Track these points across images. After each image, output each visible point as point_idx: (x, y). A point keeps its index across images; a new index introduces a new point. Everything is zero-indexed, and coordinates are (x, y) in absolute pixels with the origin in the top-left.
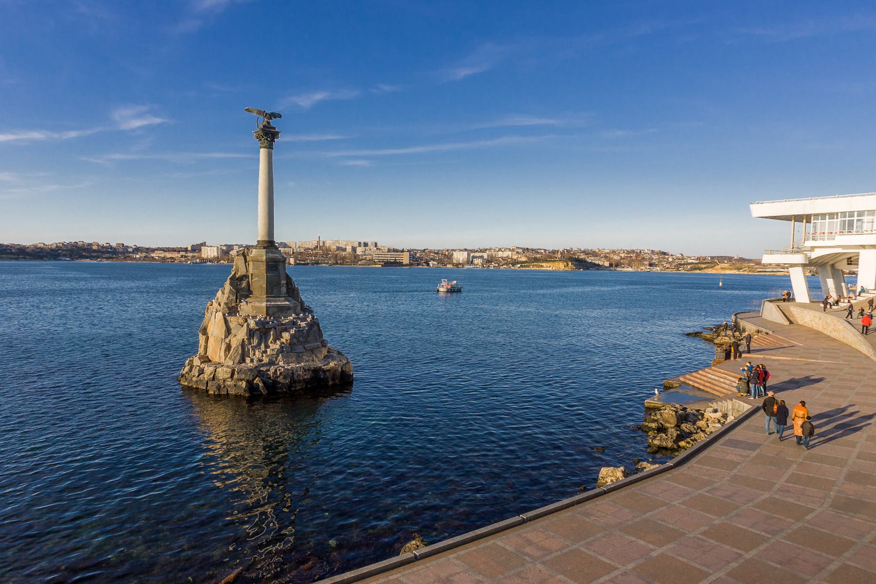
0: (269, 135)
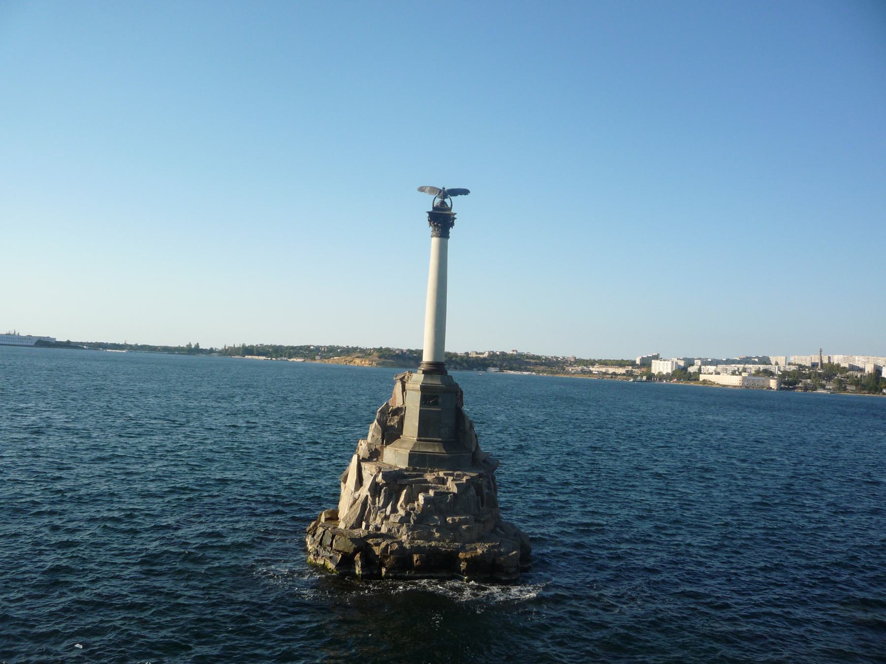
0: (442, 221)
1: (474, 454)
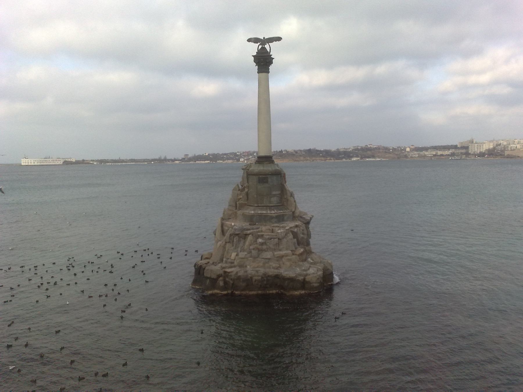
0: (263, 61)
1: (293, 213)
